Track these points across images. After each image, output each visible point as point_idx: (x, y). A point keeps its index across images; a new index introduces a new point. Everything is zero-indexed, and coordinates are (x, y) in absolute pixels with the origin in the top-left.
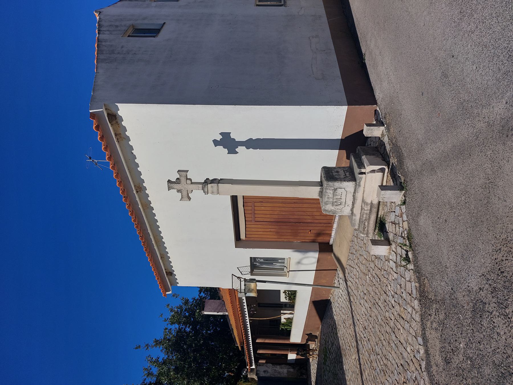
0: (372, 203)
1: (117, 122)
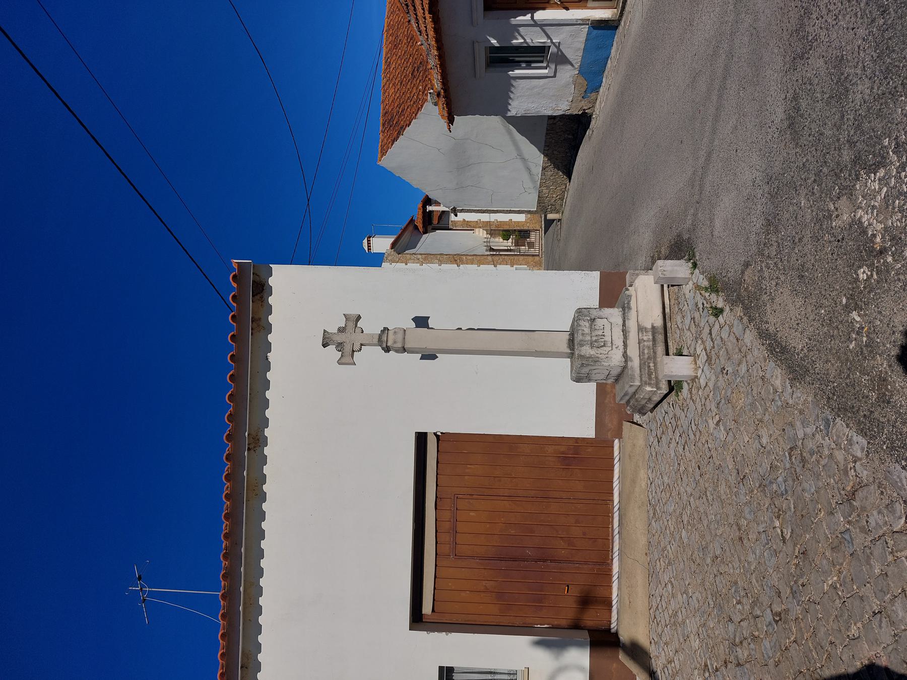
0: (653, 327)
1: (262, 297)
